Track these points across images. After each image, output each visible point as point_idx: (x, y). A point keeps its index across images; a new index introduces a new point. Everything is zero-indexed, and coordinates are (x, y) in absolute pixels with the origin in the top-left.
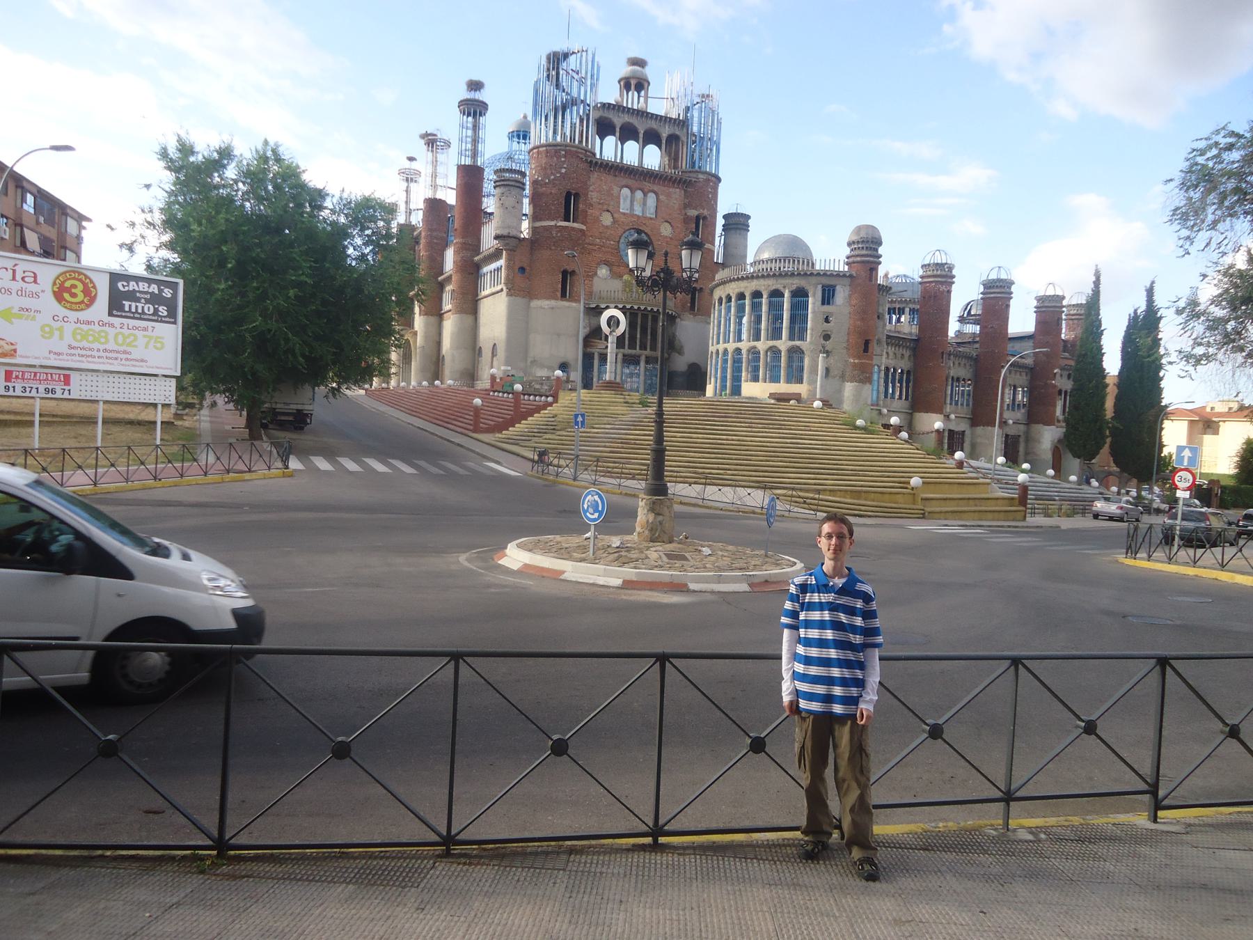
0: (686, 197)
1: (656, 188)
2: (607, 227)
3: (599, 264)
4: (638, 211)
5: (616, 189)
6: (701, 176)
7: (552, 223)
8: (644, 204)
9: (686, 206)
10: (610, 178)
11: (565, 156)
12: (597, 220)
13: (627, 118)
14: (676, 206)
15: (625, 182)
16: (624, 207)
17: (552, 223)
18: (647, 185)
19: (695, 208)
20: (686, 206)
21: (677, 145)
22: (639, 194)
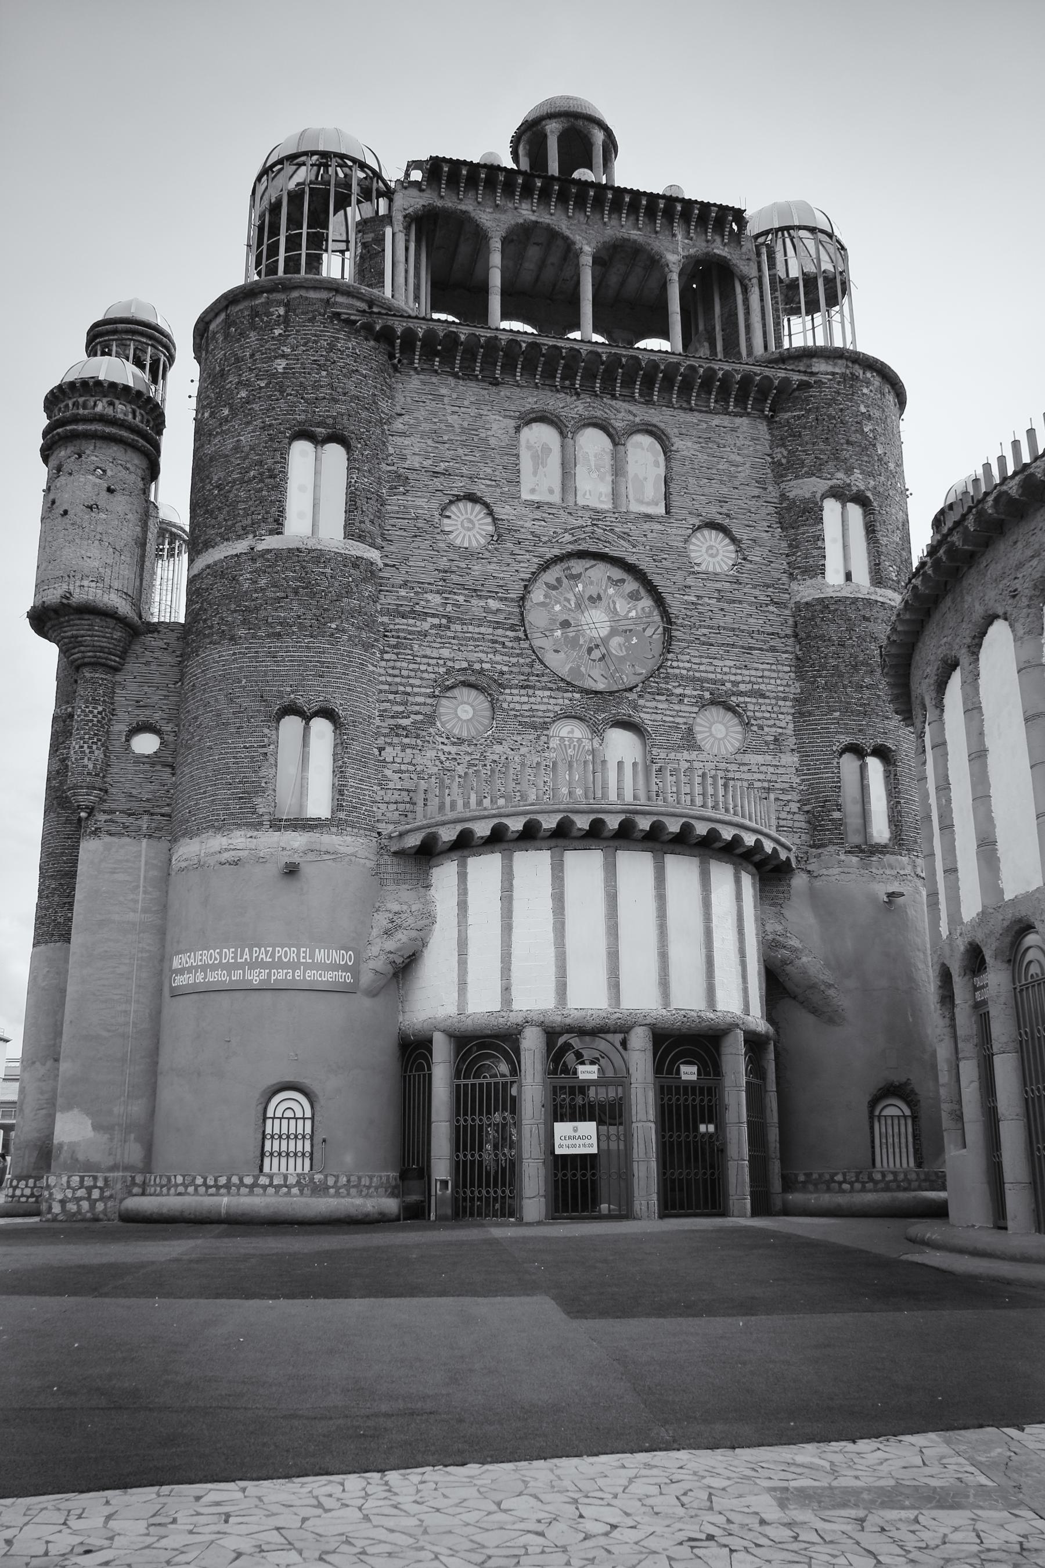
0: (778, 441)
1: (656, 416)
2: (468, 554)
3: (444, 688)
4: (593, 490)
5: (498, 426)
6: (820, 366)
7: (241, 546)
8: (618, 469)
9: (781, 471)
10: (472, 391)
11: (286, 321)
12: (428, 530)
13: (527, 212)
14: (745, 472)
15: (532, 400)
16: (539, 482)
17: (241, 546)
18: (622, 412)
19: (816, 471)
20: (781, 471)
21: (728, 297)
22: (592, 443)
